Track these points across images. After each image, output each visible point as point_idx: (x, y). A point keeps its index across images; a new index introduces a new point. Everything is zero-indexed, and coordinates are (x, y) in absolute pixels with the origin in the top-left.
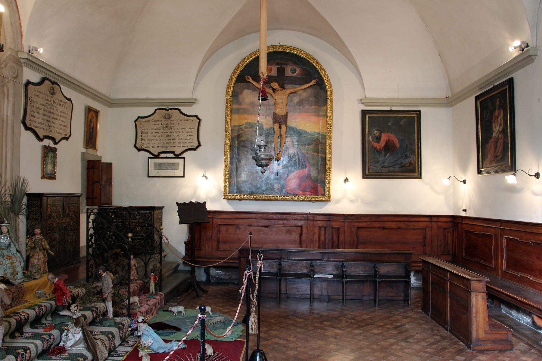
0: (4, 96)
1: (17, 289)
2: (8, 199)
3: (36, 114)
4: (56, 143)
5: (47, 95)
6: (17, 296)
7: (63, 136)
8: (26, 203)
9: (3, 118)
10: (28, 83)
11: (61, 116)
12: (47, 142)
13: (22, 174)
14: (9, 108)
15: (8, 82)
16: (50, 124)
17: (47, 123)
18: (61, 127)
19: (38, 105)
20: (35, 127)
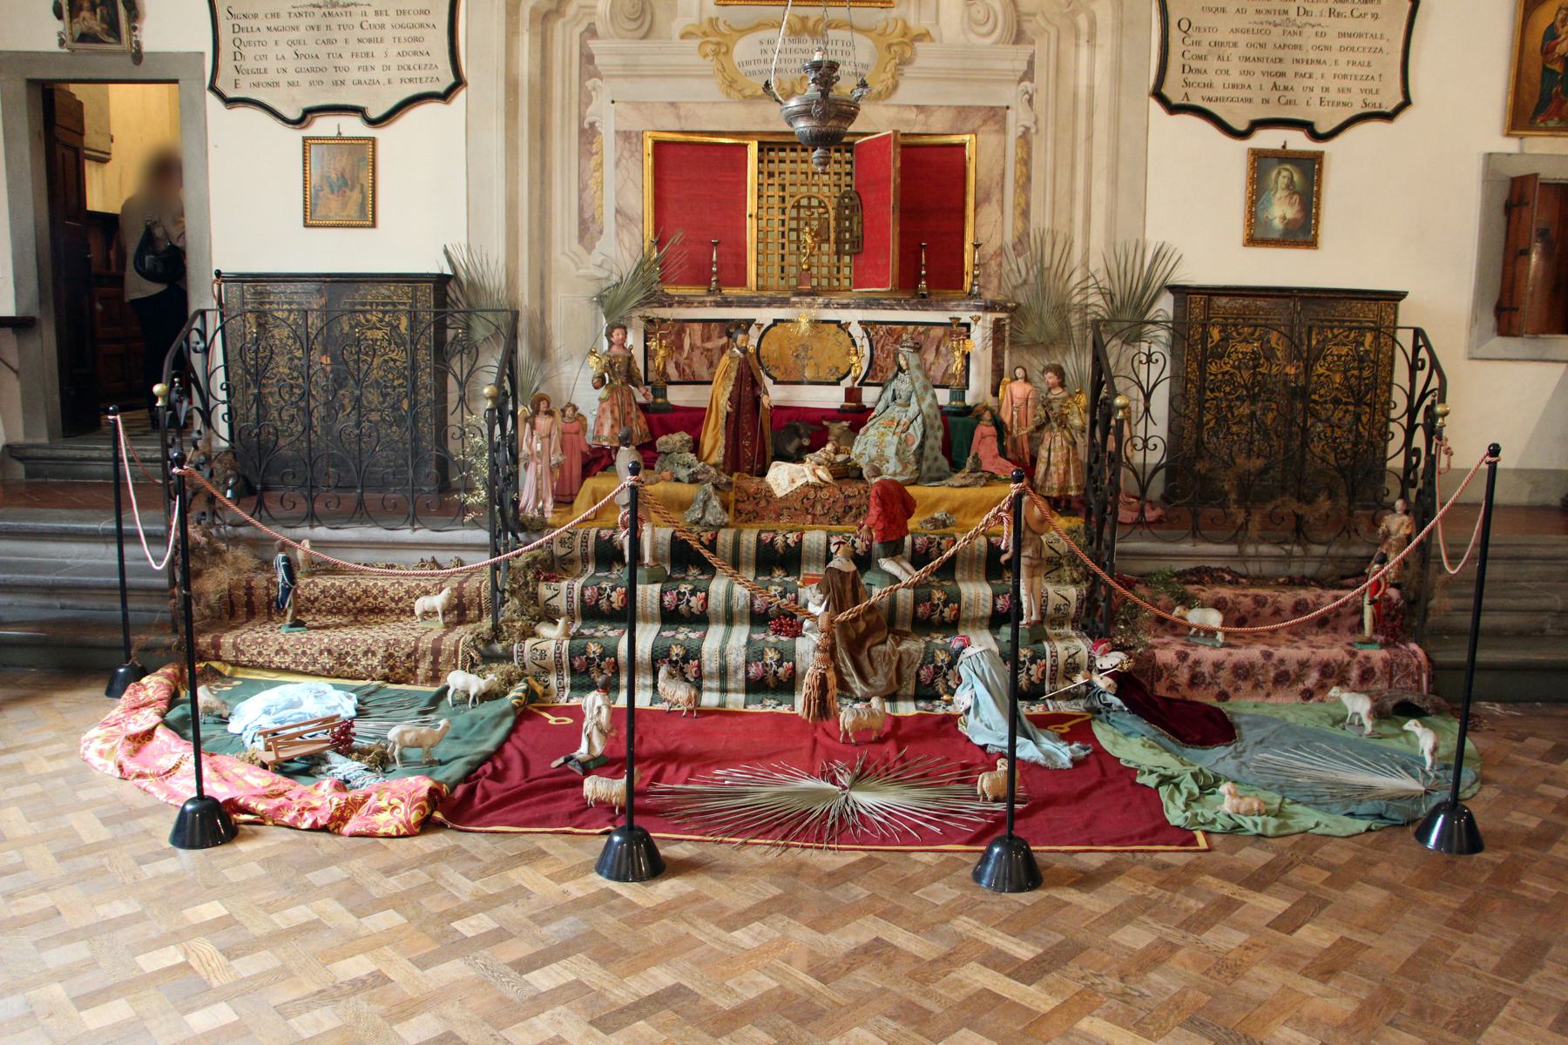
0: (1077, 37)
3: (1213, 64)
4: (1316, 136)
7: (1358, 110)
9: (1075, 95)
12: (1268, 139)
13: (1153, 239)
14: (1098, 67)
16: (1281, 82)
17: (1268, 83)
18: (1345, 83)
20: (1210, 100)
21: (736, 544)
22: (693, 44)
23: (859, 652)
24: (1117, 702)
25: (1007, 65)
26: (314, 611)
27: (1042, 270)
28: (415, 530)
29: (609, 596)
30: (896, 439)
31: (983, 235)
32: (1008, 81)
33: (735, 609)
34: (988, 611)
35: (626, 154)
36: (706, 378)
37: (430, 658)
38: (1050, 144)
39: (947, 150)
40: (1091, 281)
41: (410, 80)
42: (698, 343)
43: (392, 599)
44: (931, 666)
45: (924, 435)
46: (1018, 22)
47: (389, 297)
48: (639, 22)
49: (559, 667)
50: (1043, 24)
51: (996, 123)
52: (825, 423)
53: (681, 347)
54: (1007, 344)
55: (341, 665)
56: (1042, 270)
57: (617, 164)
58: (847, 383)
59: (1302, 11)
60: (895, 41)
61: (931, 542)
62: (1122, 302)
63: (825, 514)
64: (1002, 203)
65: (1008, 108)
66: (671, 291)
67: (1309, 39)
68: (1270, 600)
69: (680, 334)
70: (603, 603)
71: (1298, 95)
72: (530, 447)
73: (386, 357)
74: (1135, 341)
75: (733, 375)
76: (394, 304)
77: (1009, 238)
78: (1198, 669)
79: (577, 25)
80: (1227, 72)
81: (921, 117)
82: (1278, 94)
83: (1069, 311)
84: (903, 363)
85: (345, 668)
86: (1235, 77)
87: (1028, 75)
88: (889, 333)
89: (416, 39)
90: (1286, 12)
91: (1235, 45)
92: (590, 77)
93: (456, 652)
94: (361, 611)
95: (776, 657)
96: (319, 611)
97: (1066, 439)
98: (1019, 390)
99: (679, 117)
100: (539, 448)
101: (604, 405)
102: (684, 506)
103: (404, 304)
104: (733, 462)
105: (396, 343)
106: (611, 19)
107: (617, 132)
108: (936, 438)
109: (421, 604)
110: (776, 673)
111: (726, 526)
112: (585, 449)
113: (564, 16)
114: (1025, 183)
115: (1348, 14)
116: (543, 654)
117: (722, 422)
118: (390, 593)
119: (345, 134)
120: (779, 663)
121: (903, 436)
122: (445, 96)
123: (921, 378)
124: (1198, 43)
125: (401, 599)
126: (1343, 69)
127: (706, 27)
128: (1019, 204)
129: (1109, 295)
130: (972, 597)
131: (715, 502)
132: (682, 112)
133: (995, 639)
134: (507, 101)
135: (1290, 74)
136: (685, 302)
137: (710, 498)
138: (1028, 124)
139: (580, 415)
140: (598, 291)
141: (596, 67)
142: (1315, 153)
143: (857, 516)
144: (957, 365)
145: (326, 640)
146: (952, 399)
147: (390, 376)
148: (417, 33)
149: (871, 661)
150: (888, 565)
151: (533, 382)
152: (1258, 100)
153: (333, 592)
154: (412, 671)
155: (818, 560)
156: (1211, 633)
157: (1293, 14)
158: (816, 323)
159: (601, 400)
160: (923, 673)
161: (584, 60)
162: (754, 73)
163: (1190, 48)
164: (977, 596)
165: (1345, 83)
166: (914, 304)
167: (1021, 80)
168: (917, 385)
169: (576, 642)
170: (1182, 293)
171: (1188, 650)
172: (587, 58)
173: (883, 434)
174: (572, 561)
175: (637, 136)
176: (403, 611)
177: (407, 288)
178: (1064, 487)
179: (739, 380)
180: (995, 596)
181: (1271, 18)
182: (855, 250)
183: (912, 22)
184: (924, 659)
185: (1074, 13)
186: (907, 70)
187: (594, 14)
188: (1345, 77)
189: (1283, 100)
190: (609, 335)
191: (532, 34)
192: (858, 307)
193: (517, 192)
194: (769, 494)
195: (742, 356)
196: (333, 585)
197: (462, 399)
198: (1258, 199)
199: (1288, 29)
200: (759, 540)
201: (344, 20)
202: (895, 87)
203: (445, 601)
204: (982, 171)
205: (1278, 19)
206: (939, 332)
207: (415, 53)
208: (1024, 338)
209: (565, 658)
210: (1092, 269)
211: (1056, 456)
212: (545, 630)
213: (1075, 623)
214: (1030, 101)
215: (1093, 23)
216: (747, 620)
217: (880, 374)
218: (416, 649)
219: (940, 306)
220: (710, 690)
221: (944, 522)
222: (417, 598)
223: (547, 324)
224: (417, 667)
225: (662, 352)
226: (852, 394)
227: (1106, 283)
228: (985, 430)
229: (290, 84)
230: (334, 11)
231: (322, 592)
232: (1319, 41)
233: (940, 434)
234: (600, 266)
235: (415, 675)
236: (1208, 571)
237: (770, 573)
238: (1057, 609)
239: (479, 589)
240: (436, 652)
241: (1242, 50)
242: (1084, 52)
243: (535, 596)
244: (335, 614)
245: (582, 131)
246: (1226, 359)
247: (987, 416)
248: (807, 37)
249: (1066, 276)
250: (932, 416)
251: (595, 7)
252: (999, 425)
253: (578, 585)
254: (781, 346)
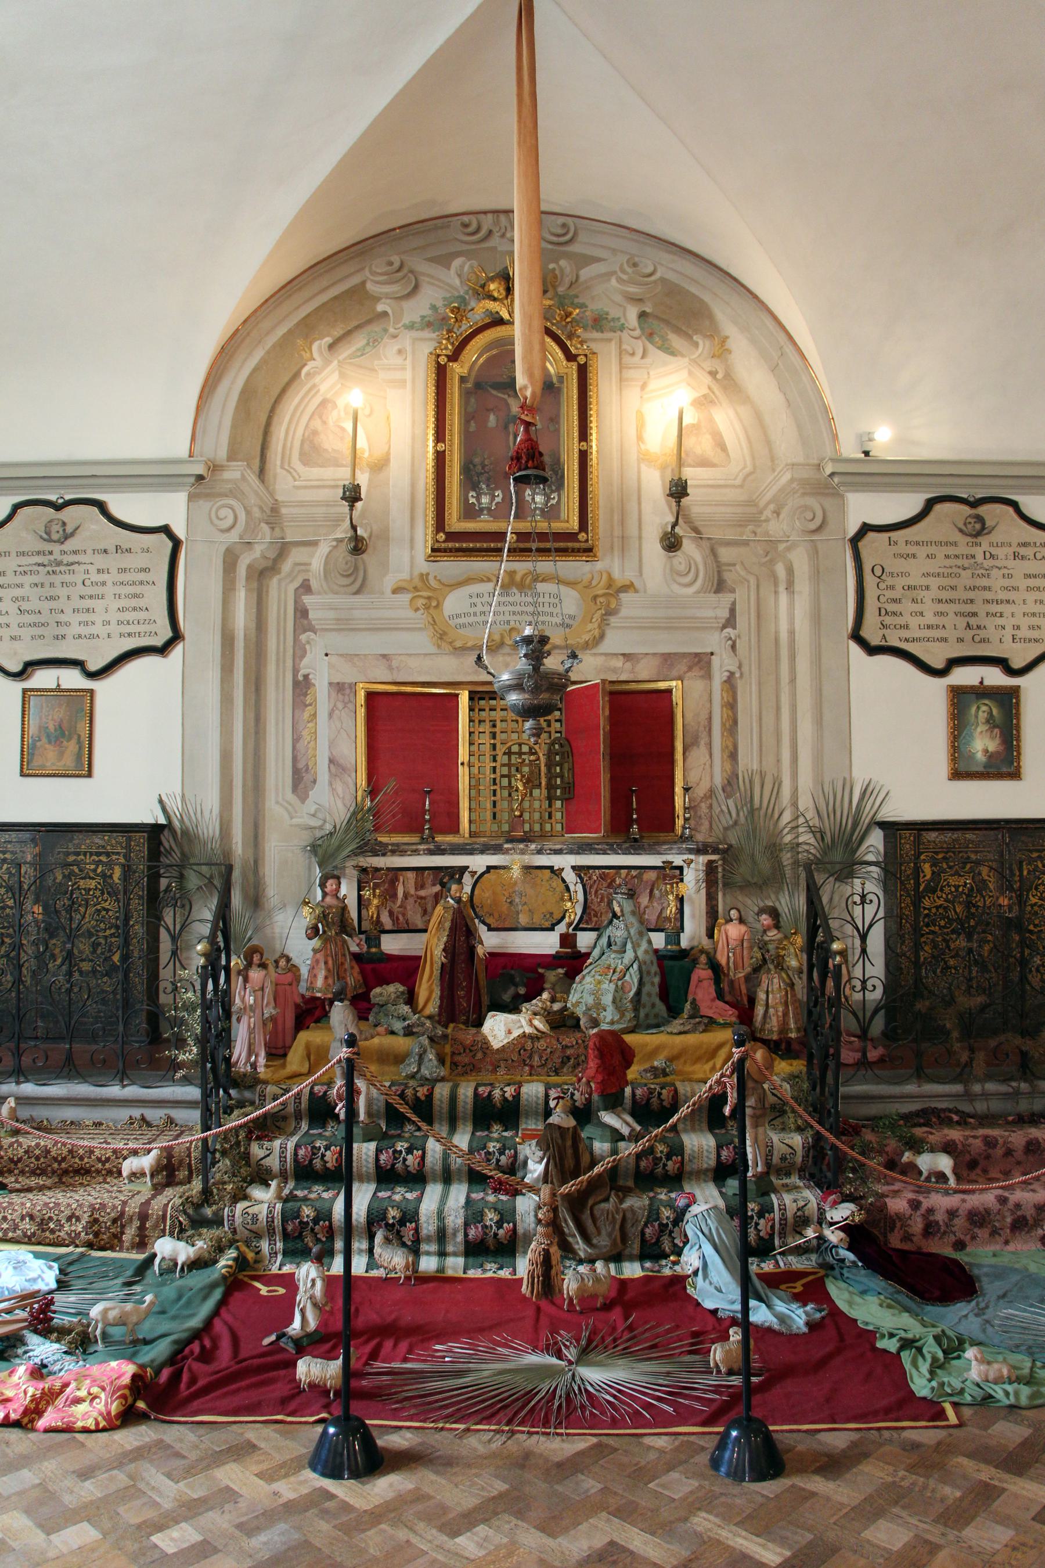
0: (776, 584)
1: (580, 1041)
2: (805, 838)
3: (907, 607)
5: (955, 544)
6: (583, 1058)
8: (881, 848)
10: (866, 528)
11: (1029, 589)
12: (966, 676)
13: (860, 776)
15: (788, 549)
16: (973, 621)
17: (961, 622)
18: (1035, 621)
19: (915, 580)
20: (907, 640)
21: (453, 1098)
22: (406, 598)
23: (582, 1212)
24: (850, 1256)
25: (710, 613)
26: (16, 1172)
27: (752, 811)
28: (124, 1086)
29: (323, 1156)
30: (612, 986)
31: (693, 779)
32: (712, 628)
33: (453, 1167)
34: (713, 1163)
35: (340, 705)
36: (420, 926)
37: (136, 1223)
38: (754, 688)
39: (654, 695)
40: (801, 820)
41: (129, 635)
42: (412, 891)
43: (99, 1160)
44: (656, 1224)
45: (641, 983)
46: (719, 572)
47: (103, 847)
48: (351, 579)
49: (271, 1231)
50: (743, 573)
51: (701, 669)
52: (540, 970)
53: (395, 895)
54: (720, 885)
55: (43, 1231)
56: (752, 811)
57: (331, 715)
58: (562, 928)
59: (988, 555)
60: (600, 592)
61: (651, 1092)
62: (833, 840)
63: (543, 1065)
64: (710, 746)
65: (712, 654)
66: (384, 839)
67: (997, 581)
68: (1001, 1141)
69: (393, 883)
70: (317, 1163)
71: (991, 633)
72: (243, 1000)
73: (99, 907)
74: (847, 878)
75: (448, 925)
76: (108, 854)
77: (718, 781)
78: (931, 1218)
79: (292, 581)
80: (921, 614)
81: (628, 665)
82: (972, 632)
83: (781, 850)
84: (617, 909)
85: (47, 1234)
86: (930, 618)
87: (731, 622)
88: (603, 877)
89: (136, 596)
90: (973, 557)
91: (927, 588)
92: (305, 631)
93: (164, 1217)
94: (66, 1172)
95: (496, 1218)
96: (22, 1172)
97: (784, 981)
98: (734, 931)
99: (390, 668)
100: (252, 1002)
101: (318, 955)
102: (399, 1059)
103: (118, 854)
104: (449, 1013)
105: (108, 893)
106: (325, 576)
107: (330, 684)
108: (653, 984)
109: (129, 1165)
110: (496, 1235)
111: (443, 1079)
112: (299, 1000)
113: (279, 573)
114: (731, 726)
115: (1032, 557)
116: (255, 1218)
117: (437, 973)
118: (97, 1153)
119: (63, 687)
120: (499, 1224)
121: (620, 983)
122: (163, 650)
123: (636, 924)
124: (892, 588)
125: (108, 1159)
126: (1032, 608)
127: (417, 582)
128: (727, 747)
129: (819, 834)
130: (696, 1149)
131: (431, 1056)
132: (395, 664)
133: (721, 1192)
134: (223, 655)
135: (982, 614)
136: (398, 850)
137: (425, 1051)
138: (733, 668)
139: (294, 966)
140: (310, 841)
141: (310, 623)
142: (1011, 687)
143: (575, 1067)
144: (672, 909)
145: (28, 1205)
146: (667, 943)
147: (102, 926)
148: (137, 589)
149: (594, 1220)
150: (608, 1118)
151: (246, 931)
152: (952, 639)
153: (37, 1152)
154: (118, 1237)
155: (537, 1114)
156: (941, 1177)
157: (980, 558)
158: (528, 869)
159: (315, 951)
160: (648, 1231)
161: (299, 614)
162: (464, 626)
163: (885, 592)
164: (701, 1147)
165: (1035, 621)
166: (627, 848)
167: (724, 627)
168: (632, 931)
169: (289, 1205)
170: (891, 828)
171: (921, 1198)
172: (302, 613)
173: (599, 982)
174: (285, 1118)
175: (351, 688)
176: (110, 1172)
177: (122, 839)
178: (784, 1029)
179: (453, 930)
180: (719, 1147)
181: (959, 562)
182: (567, 796)
183: (616, 574)
184: (649, 1216)
185: (772, 562)
186: (613, 620)
187: (308, 571)
188: (1034, 615)
189: (977, 639)
190: (323, 885)
191: (248, 590)
192: (571, 852)
193: (232, 742)
194: (486, 1044)
195: (456, 906)
196: (38, 1145)
197: (174, 953)
198: (959, 735)
199: (977, 572)
200: (476, 1094)
201: (67, 578)
202: (602, 636)
203: (153, 1163)
204: (689, 716)
205: (966, 563)
206: (652, 875)
207: (135, 609)
208: (738, 879)
209: (278, 1222)
210: (801, 808)
211: (774, 998)
212: (257, 1193)
213: (802, 1172)
214: (733, 647)
215: (790, 571)
216: (465, 1178)
217: (595, 919)
218: (122, 1213)
219: (652, 850)
220: (428, 1253)
221: (664, 1070)
222: (125, 1158)
223: (261, 874)
224: (123, 1233)
225: (375, 902)
226: (567, 940)
227: (815, 822)
228: (702, 973)
229: (13, 638)
230: (58, 569)
231: (26, 1152)
232: (1007, 582)
233: (657, 980)
234: (314, 815)
235: (121, 1241)
236: (935, 1112)
237: (488, 1128)
238: (783, 1158)
239: (189, 1149)
240: (143, 1217)
241: (934, 593)
242: (783, 598)
243: (246, 1156)
244: (39, 1175)
245: (296, 684)
246: (939, 893)
247: (703, 959)
248: (515, 590)
249: (776, 816)
250: (648, 962)
251: (310, 564)
252: (715, 967)
253: (291, 1145)
254: (494, 893)
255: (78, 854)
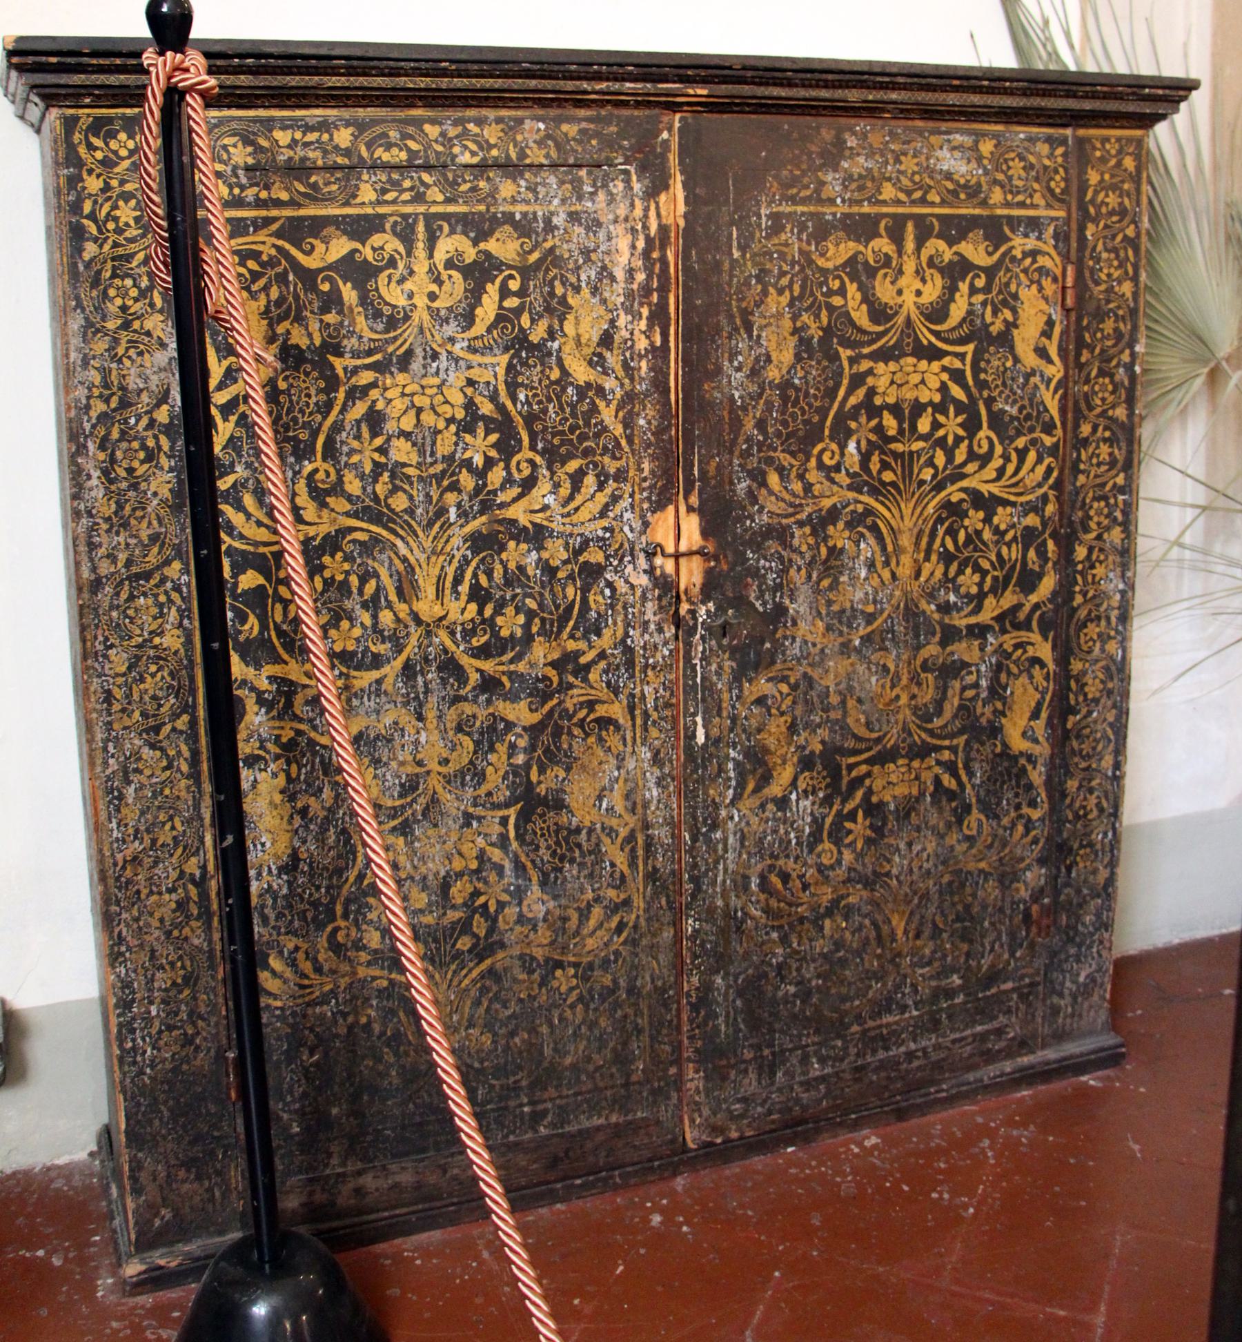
47: (973, 192)
73: (954, 493)
76: (995, 231)
103: (1034, 224)
105: (997, 421)
147: (969, 581)
255: (863, 228)
